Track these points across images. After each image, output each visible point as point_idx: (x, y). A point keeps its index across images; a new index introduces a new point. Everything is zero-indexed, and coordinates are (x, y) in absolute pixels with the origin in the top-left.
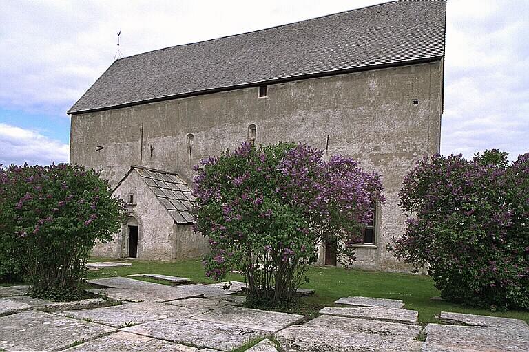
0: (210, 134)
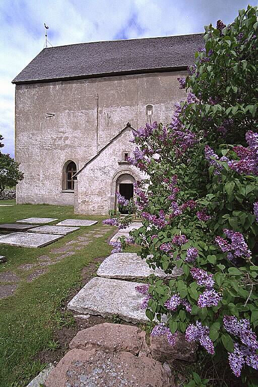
0: (170, 106)
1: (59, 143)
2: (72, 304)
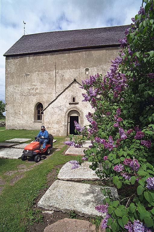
1: (33, 91)
2: (41, 203)
